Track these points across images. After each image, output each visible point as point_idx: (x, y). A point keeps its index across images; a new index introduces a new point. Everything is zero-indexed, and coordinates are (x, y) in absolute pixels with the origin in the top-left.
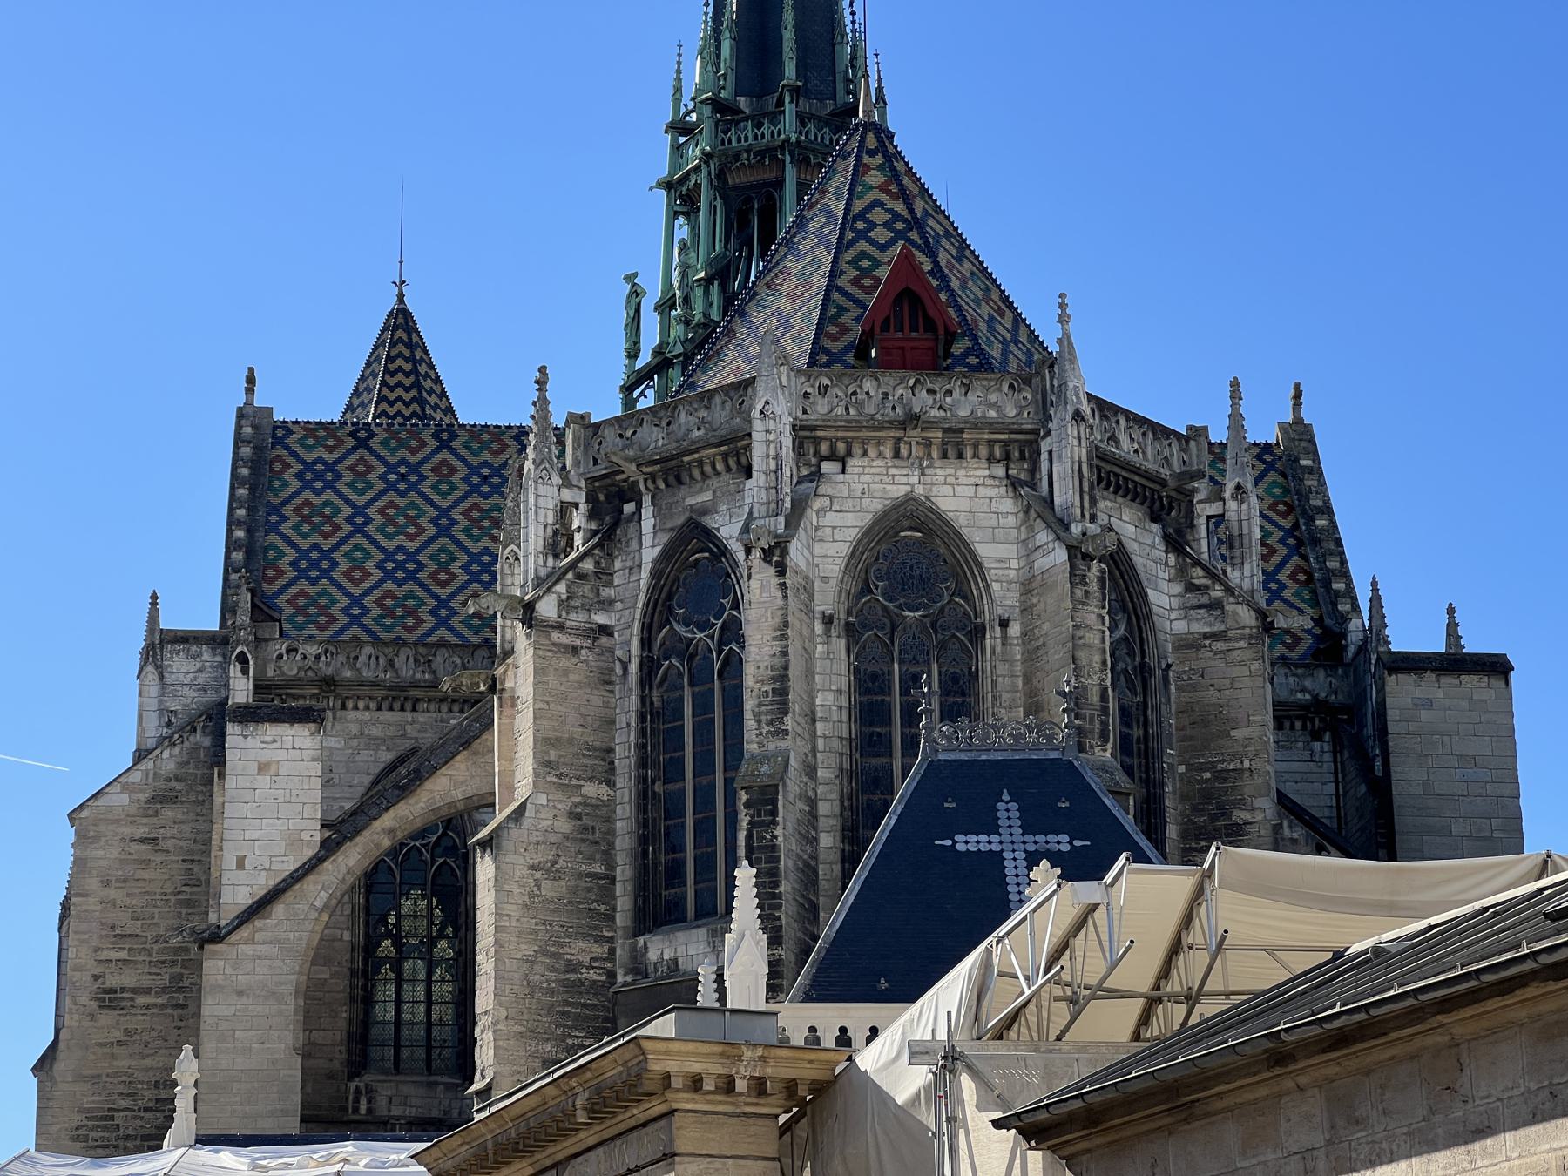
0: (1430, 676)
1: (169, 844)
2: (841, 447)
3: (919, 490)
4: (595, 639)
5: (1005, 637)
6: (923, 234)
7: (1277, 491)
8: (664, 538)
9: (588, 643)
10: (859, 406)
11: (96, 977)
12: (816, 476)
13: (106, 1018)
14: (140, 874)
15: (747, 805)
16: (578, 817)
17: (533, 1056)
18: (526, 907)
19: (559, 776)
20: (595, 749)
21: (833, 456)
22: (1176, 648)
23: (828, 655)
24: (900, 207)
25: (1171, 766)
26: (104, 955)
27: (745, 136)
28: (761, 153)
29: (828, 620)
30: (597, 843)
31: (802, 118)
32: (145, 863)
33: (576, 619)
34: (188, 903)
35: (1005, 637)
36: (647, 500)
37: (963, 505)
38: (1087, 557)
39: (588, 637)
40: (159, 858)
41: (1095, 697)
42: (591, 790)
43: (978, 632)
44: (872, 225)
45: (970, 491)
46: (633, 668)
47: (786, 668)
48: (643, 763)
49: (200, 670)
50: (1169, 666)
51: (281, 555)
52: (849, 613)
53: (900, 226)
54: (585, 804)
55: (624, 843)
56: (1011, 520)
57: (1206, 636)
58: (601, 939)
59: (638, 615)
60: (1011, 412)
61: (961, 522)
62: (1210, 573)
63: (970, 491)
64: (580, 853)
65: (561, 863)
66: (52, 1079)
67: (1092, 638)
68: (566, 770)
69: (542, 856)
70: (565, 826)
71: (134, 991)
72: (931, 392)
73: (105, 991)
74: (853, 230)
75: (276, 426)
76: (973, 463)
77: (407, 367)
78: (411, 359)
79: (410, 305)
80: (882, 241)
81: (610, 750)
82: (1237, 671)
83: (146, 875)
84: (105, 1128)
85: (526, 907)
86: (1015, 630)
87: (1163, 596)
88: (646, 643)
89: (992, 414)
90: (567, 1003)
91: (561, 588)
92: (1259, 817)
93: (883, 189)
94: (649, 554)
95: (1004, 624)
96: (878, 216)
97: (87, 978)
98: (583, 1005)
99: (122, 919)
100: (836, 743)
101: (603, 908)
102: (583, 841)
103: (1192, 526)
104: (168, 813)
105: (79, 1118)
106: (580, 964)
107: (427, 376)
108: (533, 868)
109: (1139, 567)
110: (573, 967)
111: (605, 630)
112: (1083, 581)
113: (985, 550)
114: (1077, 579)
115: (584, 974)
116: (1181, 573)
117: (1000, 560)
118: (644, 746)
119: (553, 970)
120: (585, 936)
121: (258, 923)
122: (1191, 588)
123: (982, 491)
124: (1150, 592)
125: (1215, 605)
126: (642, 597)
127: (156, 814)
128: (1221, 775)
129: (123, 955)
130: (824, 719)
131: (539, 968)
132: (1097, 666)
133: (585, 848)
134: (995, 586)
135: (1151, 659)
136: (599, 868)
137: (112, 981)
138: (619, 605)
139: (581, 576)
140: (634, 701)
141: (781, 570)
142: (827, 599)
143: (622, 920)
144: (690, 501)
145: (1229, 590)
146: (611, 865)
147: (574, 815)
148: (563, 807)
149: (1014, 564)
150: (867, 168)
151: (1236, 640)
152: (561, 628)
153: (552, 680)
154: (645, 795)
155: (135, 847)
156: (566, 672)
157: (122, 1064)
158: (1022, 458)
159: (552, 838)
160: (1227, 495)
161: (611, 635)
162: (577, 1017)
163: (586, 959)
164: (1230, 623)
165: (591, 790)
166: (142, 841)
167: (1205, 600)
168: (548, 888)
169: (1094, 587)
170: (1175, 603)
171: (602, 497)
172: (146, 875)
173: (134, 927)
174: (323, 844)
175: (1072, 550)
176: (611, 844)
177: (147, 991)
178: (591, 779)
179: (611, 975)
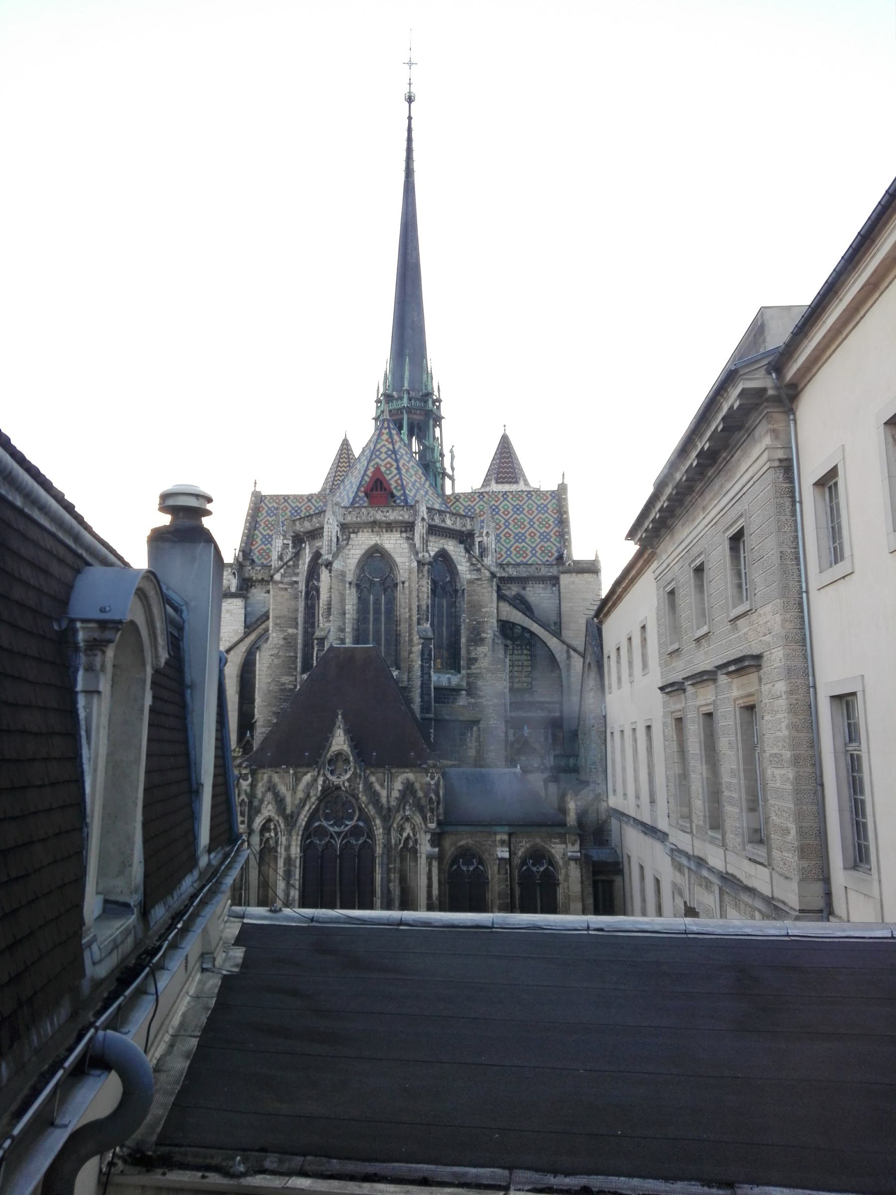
0: (574, 574)
2: (356, 530)
3: (379, 542)
5: (403, 587)
6: (396, 456)
7: (554, 506)
8: (311, 555)
10: (360, 517)
12: (349, 538)
15: (317, 644)
17: (270, 711)
18: (268, 667)
21: (354, 532)
22: (467, 583)
23: (350, 594)
24: (391, 447)
25: (464, 620)
27: (395, 405)
28: (398, 410)
29: (350, 583)
31: (410, 399)
33: (286, 580)
35: (403, 587)
36: (307, 543)
37: (392, 546)
38: (424, 565)
41: (424, 608)
42: (290, 631)
43: (396, 585)
44: (381, 453)
45: (394, 542)
46: (303, 594)
47: (331, 601)
50: (464, 590)
51: (258, 537)
52: (358, 580)
53: (390, 453)
56: (407, 550)
57: (476, 579)
58: (292, 675)
60: (406, 517)
61: (391, 552)
62: (477, 560)
63: (394, 542)
65: (280, 654)
67: (424, 589)
69: (275, 652)
70: (282, 642)
72: (382, 511)
74: (375, 455)
75: (262, 496)
76: (396, 533)
77: (346, 456)
78: (348, 454)
79: (348, 438)
80: (383, 458)
81: (297, 618)
82: (485, 590)
86: (406, 584)
88: (307, 586)
89: (401, 518)
91: (282, 571)
92: (489, 636)
93: (387, 441)
94: (308, 560)
95: (403, 583)
96: (384, 450)
100: (352, 621)
101: (293, 666)
103: (474, 544)
106: (285, 683)
107: (352, 459)
108: (272, 655)
110: (283, 684)
111: (296, 582)
112: (422, 572)
113: (398, 560)
114: (419, 571)
115: (287, 686)
116: (469, 560)
117: (402, 563)
122: (472, 564)
123: (398, 542)
125: (479, 570)
128: (478, 623)
130: (349, 613)
131: (272, 685)
132: (425, 598)
134: (401, 571)
135: (458, 587)
136: (292, 654)
139: (288, 567)
141: (330, 571)
142: (350, 577)
143: (299, 669)
144: (317, 545)
145: (483, 565)
146: (296, 653)
147: (285, 639)
149: (407, 564)
150: (383, 434)
152: (282, 582)
156: (283, 596)
158: (411, 531)
159: (277, 646)
160: (484, 535)
162: (284, 699)
163: (287, 681)
164: (483, 575)
165: (290, 631)
168: (276, 661)
169: (426, 573)
170: (467, 569)
174: (245, 633)
175: (419, 562)
176: (297, 647)
178: (291, 627)
179: (295, 686)
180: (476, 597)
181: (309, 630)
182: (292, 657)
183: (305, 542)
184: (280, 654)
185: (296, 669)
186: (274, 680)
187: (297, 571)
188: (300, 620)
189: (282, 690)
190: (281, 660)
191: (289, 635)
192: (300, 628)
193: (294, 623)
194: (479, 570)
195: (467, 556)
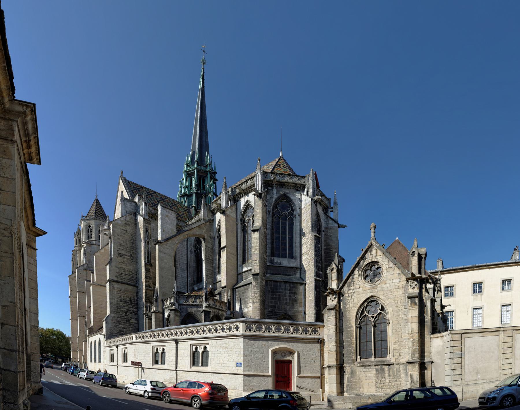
1: (129, 232)
11: (118, 251)
13: (120, 258)
14: (124, 235)
26: (119, 247)
32: (125, 234)
34: (133, 243)
40: (128, 234)
46: (271, 213)
49: (132, 206)
66: (111, 265)
71: (124, 255)
73: (119, 253)
83: (125, 236)
84: (121, 276)
97: (117, 251)
99: (122, 242)
104: (128, 227)
105: (116, 274)
126: (273, 203)
127: (126, 226)
129: (122, 248)
137: (120, 252)
155: (123, 231)
157: (123, 266)
166: (124, 230)
172: (125, 236)
173: (123, 244)
177: (126, 255)
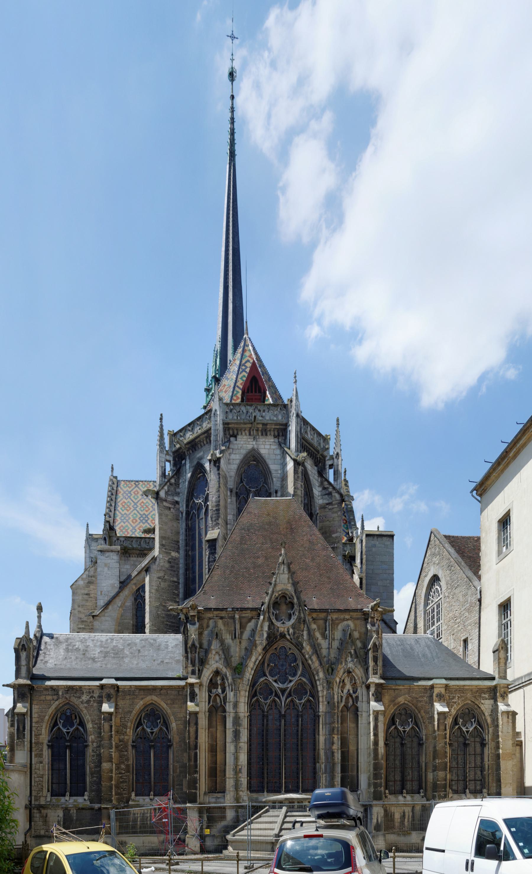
4: (175, 505)
9: (173, 506)
16: (170, 562)
19: (165, 549)
20: (175, 541)
22: (320, 508)
30: (175, 571)
33: (170, 498)
39: (172, 504)
48: (186, 545)
50: (318, 514)
54: (172, 559)
55: (181, 571)
57: (327, 504)
59: (185, 497)
64: (171, 574)
65: (166, 577)
68: (167, 547)
70: (167, 565)
82: (336, 515)
85: (157, 590)
87: (317, 491)
88: (187, 506)
90: (167, 621)
91: (166, 488)
98: (172, 622)
101: (176, 592)
102: (172, 570)
109: (311, 480)
111: (177, 503)
116: (321, 484)
118: (186, 540)
119: (164, 610)
120: (172, 601)
121: (106, 611)
122: (324, 488)
124: (314, 489)
125: (330, 494)
133: (172, 573)
138: (181, 494)
139: (171, 484)
140: (184, 524)
143: (181, 596)
147: (169, 562)
148: (167, 559)
151: (335, 505)
153: (164, 518)
154: (187, 555)
156: (167, 516)
159: (164, 569)
161: (179, 504)
162: (170, 626)
164: (333, 499)
165: (174, 554)
167: (327, 492)
168: (163, 585)
170: (320, 494)
171: (177, 459)
178: (173, 551)
180: (328, 523)
181: (190, 553)
182: (174, 582)
183: (185, 459)
184: (166, 577)
185: (178, 595)
186: (161, 605)
187: (178, 490)
188: (182, 543)
189: (169, 616)
190: (167, 584)
191: (172, 558)
192: (182, 552)
193: (177, 546)
194: (330, 494)
195: (319, 480)
